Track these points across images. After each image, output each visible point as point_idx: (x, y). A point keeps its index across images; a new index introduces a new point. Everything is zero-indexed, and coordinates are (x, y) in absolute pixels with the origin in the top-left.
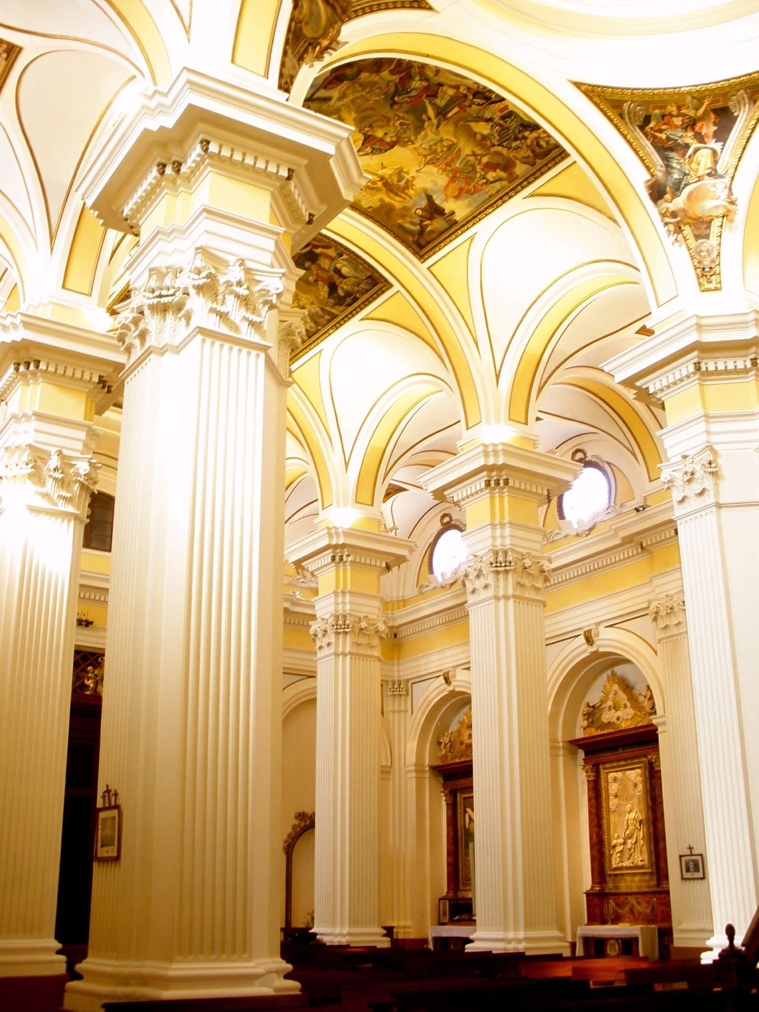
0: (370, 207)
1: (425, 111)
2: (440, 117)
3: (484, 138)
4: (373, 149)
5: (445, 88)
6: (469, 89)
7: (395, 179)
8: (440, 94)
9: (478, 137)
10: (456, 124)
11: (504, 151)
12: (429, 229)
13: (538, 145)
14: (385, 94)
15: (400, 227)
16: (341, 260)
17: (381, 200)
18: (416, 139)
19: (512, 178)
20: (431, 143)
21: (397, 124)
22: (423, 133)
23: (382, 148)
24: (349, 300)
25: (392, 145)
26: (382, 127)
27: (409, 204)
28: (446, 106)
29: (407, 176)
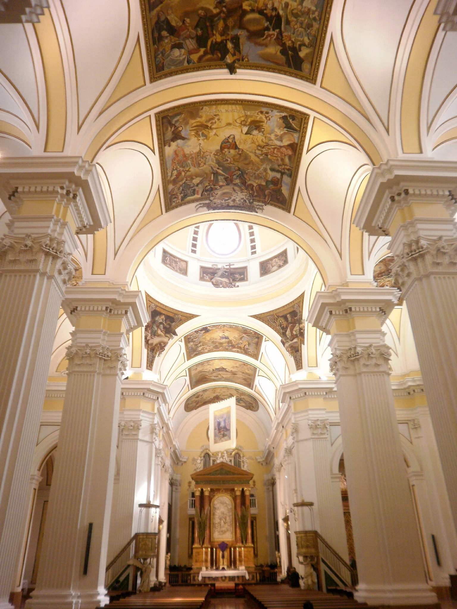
0: (202, 109)
1: (222, 170)
2: (215, 172)
3: (193, 179)
4: (228, 142)
5: (224, 184)
6: (216, 189)
7: (205, 133)
8: (224, 180)
9: (194, 177)
10: (206, 174)
11: (181, 183)
12: (169, 128)
13: (175, 198)
14: (247, 174)
15: (180, 114)
16: (184, 59)
17: (201, 117)
18: (215, 157)
19: (169, 182)
20: (207, 160)
21: (229, 160)
22: (215, 161)
23: (225, 144)
24: (156, 35)
25: (222, 148)
26: (234, 156)
27: (188, 128)
28: (217, 178)
29: (202, 138)
